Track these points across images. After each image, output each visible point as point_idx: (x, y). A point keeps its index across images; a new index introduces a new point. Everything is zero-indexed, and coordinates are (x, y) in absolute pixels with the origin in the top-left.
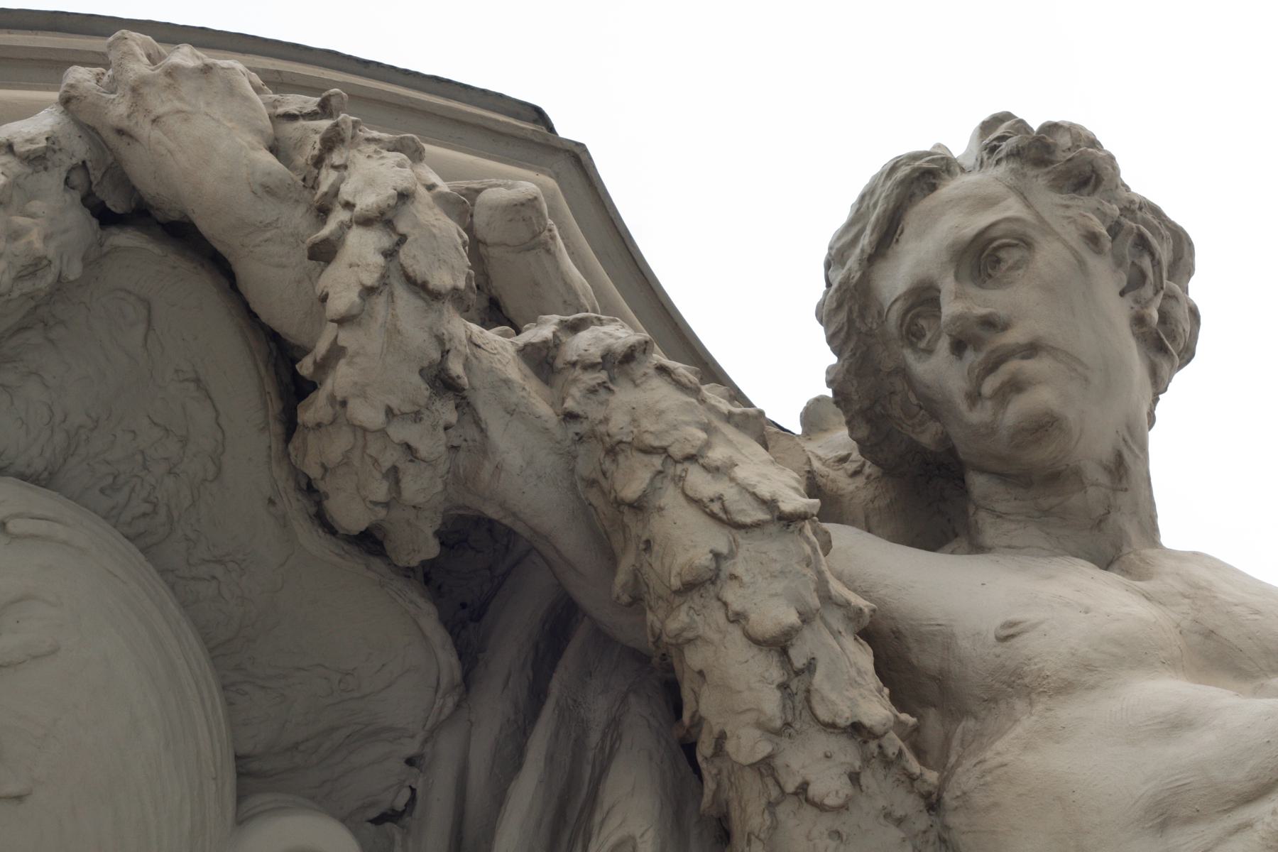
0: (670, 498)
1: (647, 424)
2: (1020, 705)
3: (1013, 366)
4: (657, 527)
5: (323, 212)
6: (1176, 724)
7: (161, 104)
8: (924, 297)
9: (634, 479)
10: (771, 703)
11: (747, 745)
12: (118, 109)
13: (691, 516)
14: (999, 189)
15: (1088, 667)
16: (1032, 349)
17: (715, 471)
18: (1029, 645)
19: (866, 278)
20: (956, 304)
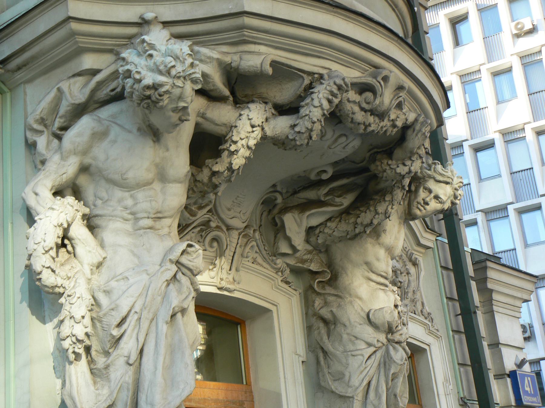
0: (387, 203)
1: (396, 197)
2: (375, 238)
3: (422, 208)
4: (383, 203)
5: (410, 158)
6: (378, 260)
7: (419, 135)
8: (430, 191)
9: (388, 198)
10: (365, 223)
11: (359, 220)
12: (417, 127)
13: (385, 208)
14: (448, 195)
15: (383, 244)
16: (425, 209)
17: (392, 208)
18: (383, 235)
19: (432, 178)
20: (430, 198)
